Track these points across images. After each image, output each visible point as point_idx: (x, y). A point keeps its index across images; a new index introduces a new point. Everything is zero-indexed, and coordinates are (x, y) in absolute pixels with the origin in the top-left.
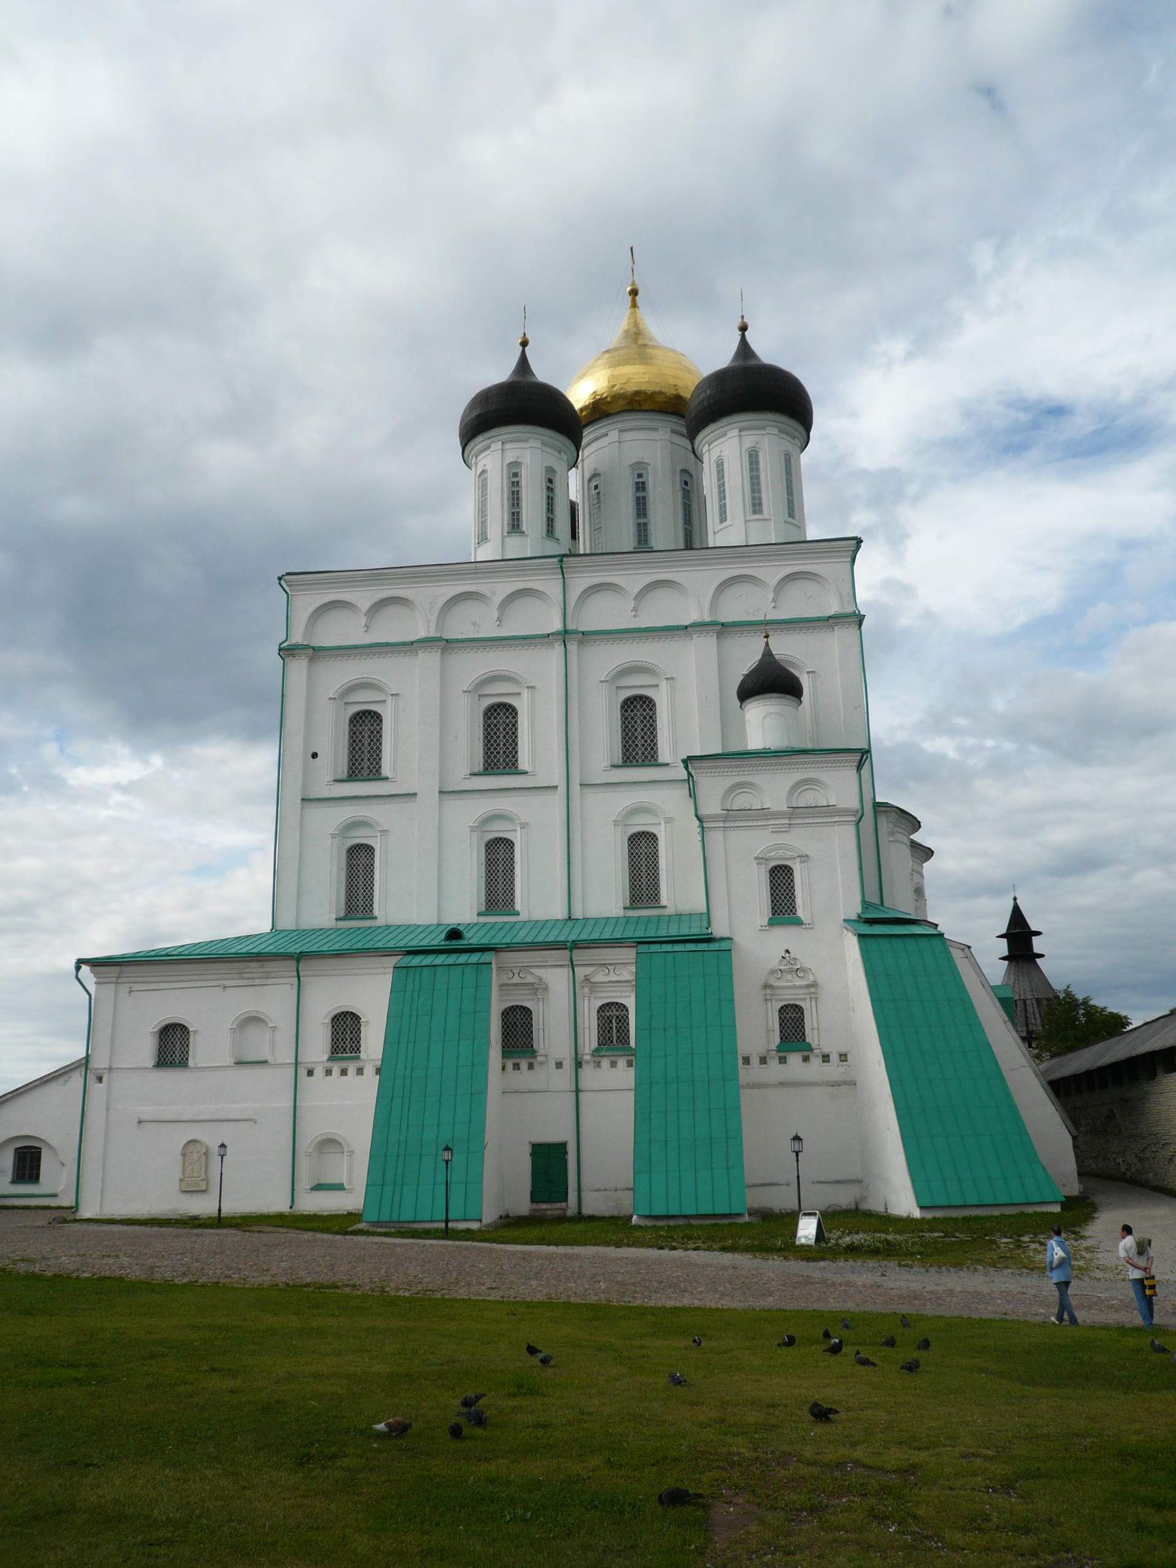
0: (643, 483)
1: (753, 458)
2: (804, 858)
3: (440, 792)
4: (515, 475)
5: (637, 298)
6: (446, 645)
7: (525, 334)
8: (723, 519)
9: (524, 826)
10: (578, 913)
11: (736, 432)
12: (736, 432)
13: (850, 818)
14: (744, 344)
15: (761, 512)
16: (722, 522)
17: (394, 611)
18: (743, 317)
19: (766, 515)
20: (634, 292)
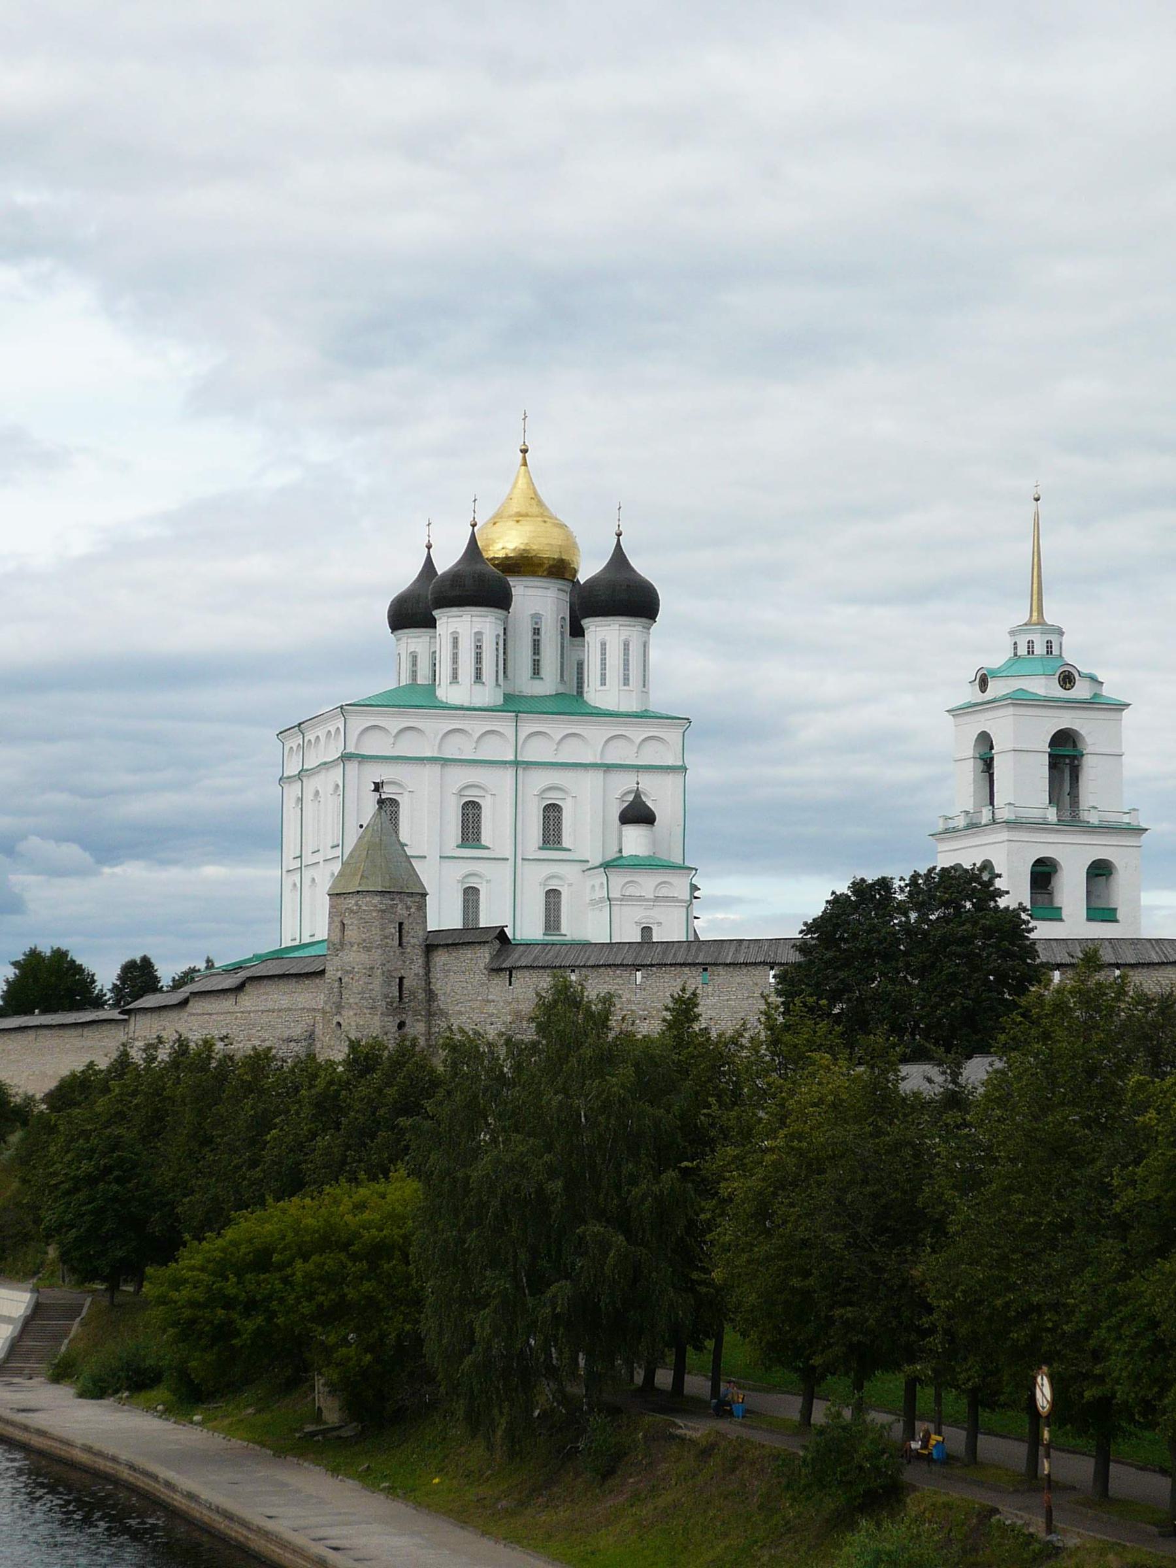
0: (538, 629)
1: (626, 645)
2: (659, 924)
3: (441, 857)
4: (479, 640)
5: (527, 454)
6: (445, 762)
7: (474, 518)
8: (603, 683)
9: (488, 881)
11: (617, 627)
12: (617, 627)
13: (684, 904)
15: (628, 685)
16: (601, 685)
17: (409, 735)
18: (619, 526)
19: (631, 688)
20: (524, 451)
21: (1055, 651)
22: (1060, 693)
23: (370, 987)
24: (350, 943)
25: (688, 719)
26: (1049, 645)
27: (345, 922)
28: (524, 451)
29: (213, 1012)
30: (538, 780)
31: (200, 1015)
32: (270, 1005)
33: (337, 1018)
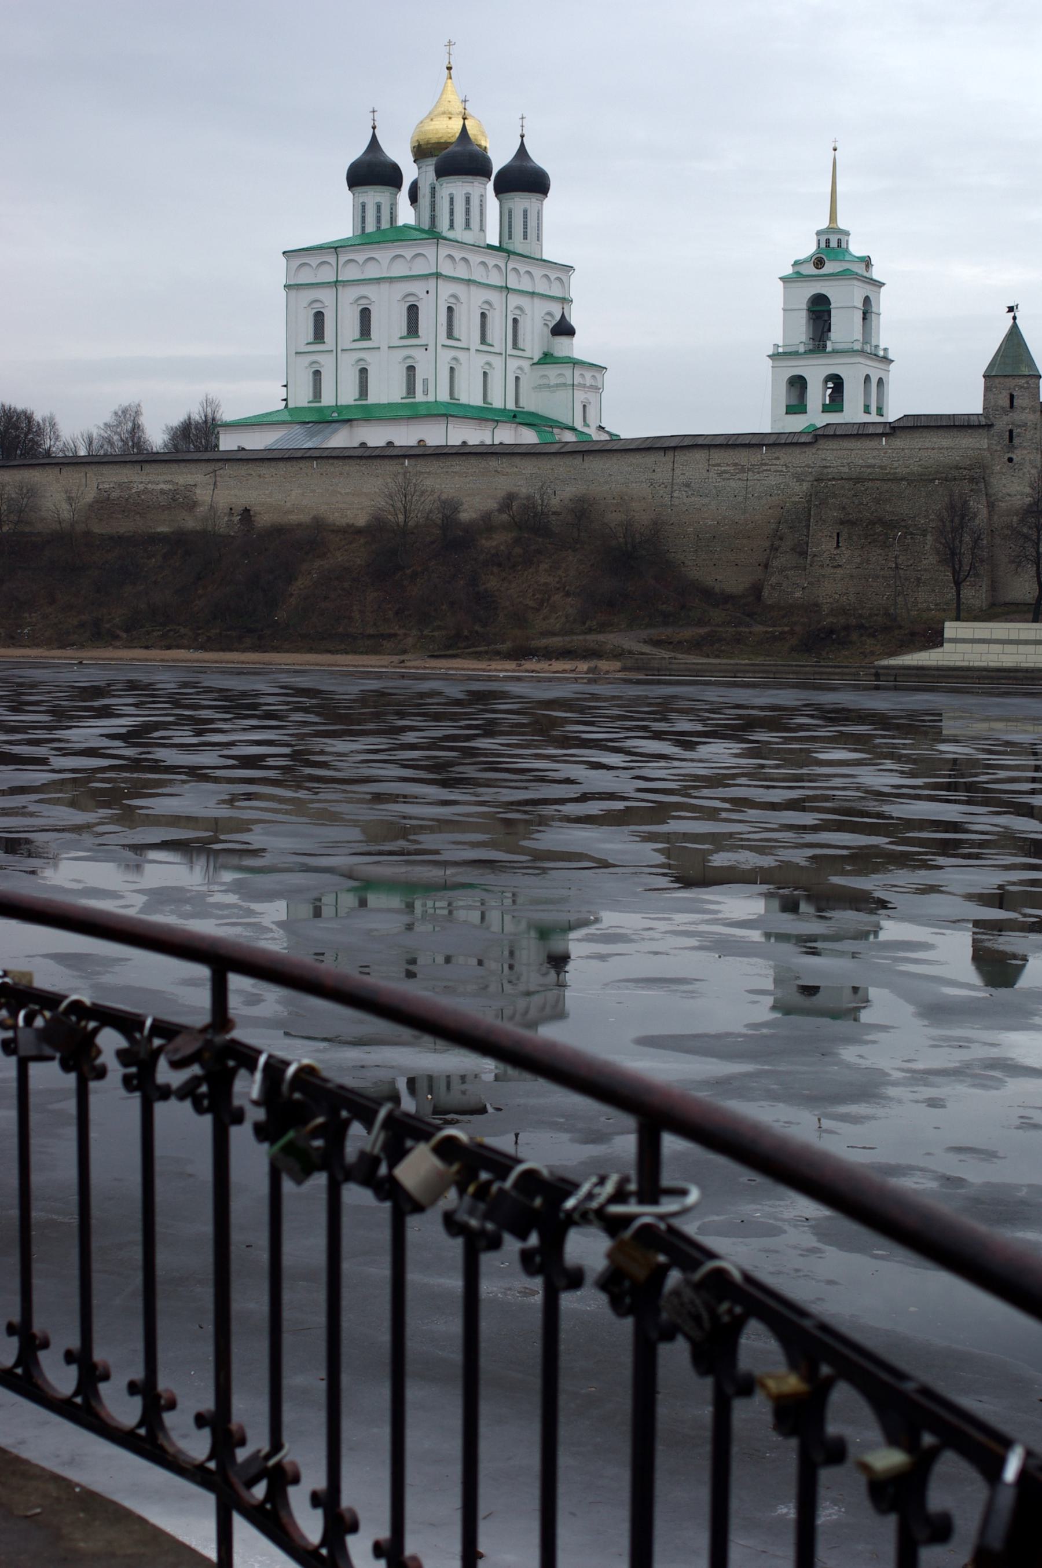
8: (525, 237)
10: (507, 408)
14: (522, 144)
16: (524, 239)
20: (449, 68)
21: (844, 245)
22: (816, 272)
23: (1036, 436)
24: (1022, 408)
25: (572, 267)
26: (839, 241)
27: (1015, 394)
28: (449, 68)
29: (855, 448)
30: (514, 300)
31: (837, 450)
32: (927, 445)
33: (1010, 455)
